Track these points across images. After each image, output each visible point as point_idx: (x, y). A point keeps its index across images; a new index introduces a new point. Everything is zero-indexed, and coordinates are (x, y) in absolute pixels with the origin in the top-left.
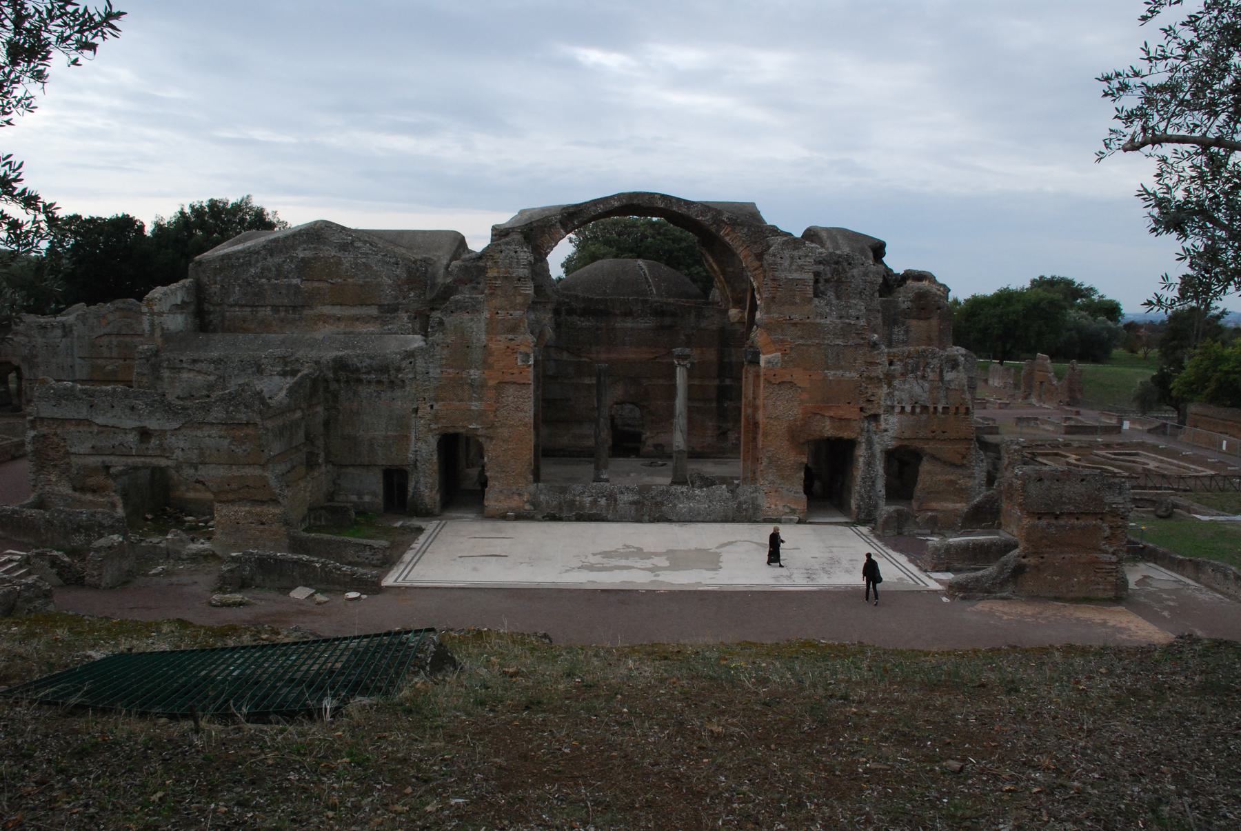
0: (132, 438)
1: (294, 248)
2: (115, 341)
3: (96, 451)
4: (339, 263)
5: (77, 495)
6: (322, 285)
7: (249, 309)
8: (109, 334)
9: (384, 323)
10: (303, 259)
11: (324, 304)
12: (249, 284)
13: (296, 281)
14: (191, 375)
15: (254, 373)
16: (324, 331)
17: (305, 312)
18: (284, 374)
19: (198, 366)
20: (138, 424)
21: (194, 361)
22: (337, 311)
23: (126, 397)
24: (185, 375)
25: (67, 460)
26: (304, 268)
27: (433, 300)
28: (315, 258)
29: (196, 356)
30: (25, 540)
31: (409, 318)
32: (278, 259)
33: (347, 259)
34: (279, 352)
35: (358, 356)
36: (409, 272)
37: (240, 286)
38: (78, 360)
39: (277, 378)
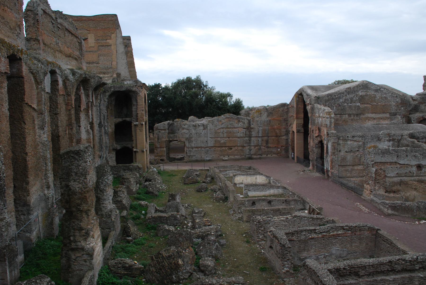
0: (414, 169)
1: (358, 91)
2: (225, 130)
3: (398, 175)
4: (375, 97)
5: (387, 194)
6: (368, 105)
7: (339, 116)
8: (222, 128)
9: (392, 120)
10: (361, 96)
11: (369, 113)
12: (340, 106)
13: (358, 104)
14: (352, 142)
15: (377, 141)
16: (369, 124)
17: (362, 116)
18: (389, 141)
19: (355, 139)
20: (418, 163)
21: (353, 137)
22: (373, 115)
23: (412, 152)
24: (349, 142)
25: (384, 180)
26: (362, 99)
27: (411, 110)
28: (366, 95)
29: (354, 134)
30: (407, 216)
31: (401, 118)
32: (351, 96)
33: (378, 95)
34: (386, 132)
35: (418, 132)
36: (401, 99)
37: (336, 107)
38: (209, 139)
39: (386, 142)
